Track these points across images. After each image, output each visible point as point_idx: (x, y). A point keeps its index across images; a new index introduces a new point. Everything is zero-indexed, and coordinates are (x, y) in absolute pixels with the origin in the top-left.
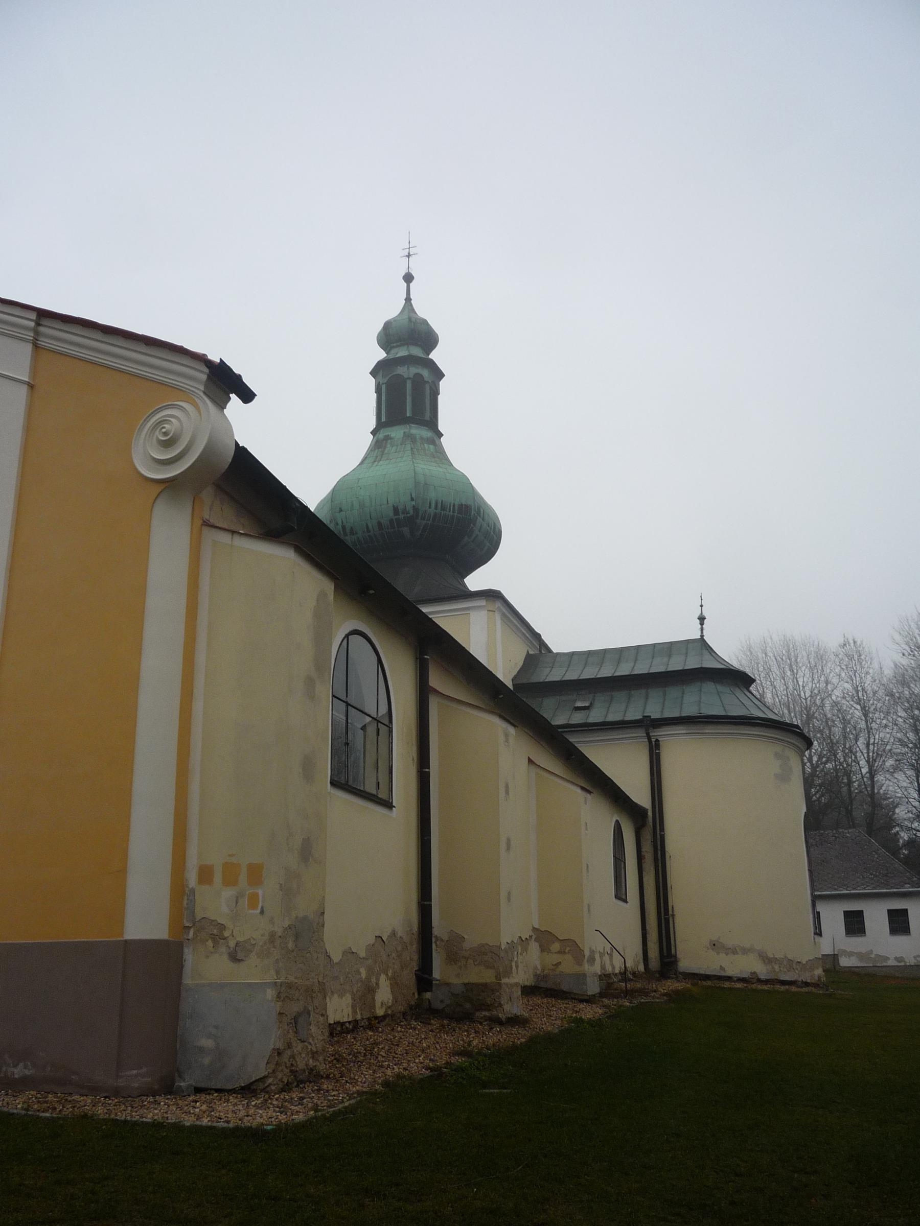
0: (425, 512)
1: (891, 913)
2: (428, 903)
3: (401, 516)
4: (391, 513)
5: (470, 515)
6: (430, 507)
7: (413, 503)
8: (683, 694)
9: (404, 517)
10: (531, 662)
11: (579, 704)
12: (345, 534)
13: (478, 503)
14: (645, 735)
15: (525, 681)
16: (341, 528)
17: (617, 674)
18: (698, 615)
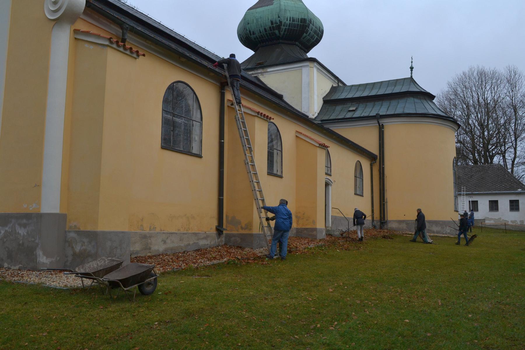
0: (285, 22)
1: (511, 202)
2: (222, 198)
3: (274, 25)
4: (270, 24)
5: (306, 23)
6: (287, 20)
7: (279, 19)
8: (398, 103)
9: (276, 26)
10: (333, 90)
11: (351, 109)
12: (251, 35)
13: (310, 17)
14: (377, 122)
15: (329, 99)
16: (249, 31)
18: (410, 66)
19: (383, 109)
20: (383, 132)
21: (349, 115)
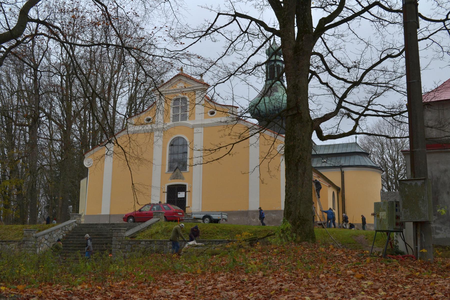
3: (276, 108)
17: (333, 153)
19: (343, 161)
20: (343, 175)
21: (324, 165)
